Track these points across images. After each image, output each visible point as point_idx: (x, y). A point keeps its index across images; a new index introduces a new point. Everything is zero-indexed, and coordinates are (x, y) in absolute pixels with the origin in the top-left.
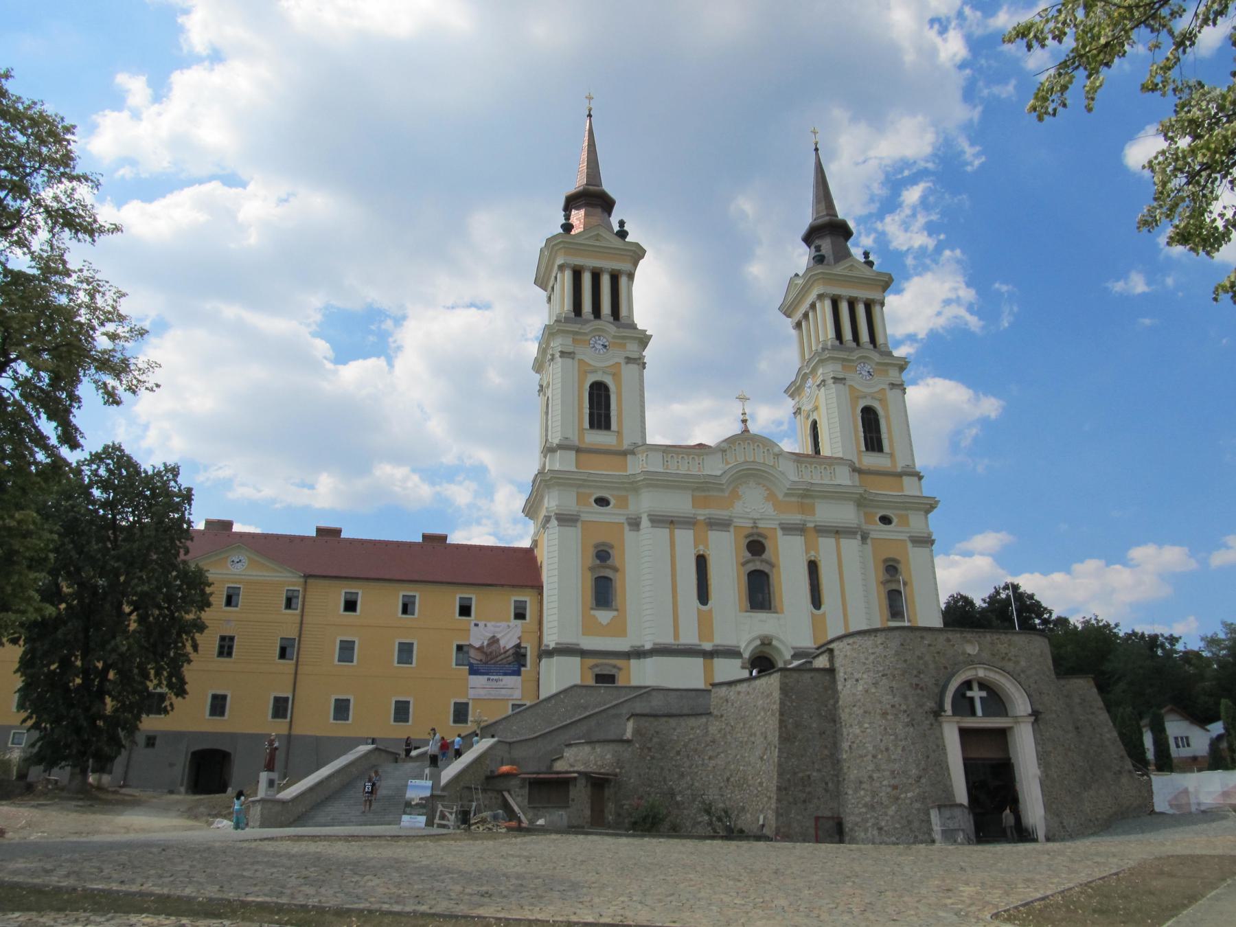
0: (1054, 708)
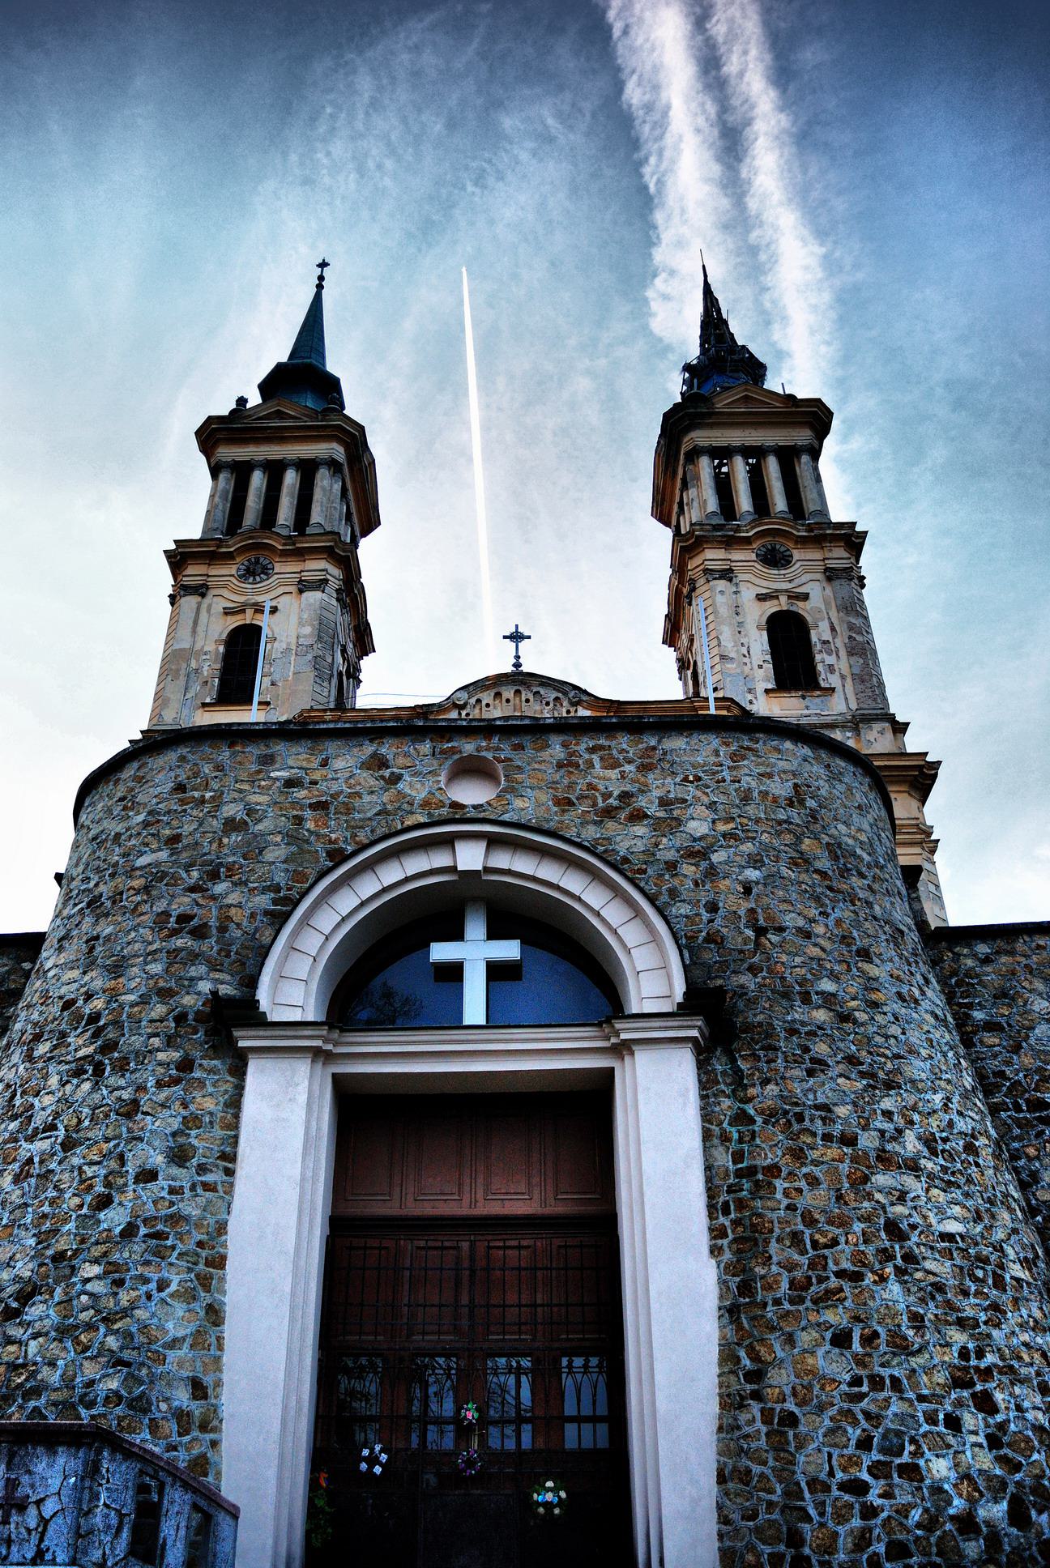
0: (827, 986)
